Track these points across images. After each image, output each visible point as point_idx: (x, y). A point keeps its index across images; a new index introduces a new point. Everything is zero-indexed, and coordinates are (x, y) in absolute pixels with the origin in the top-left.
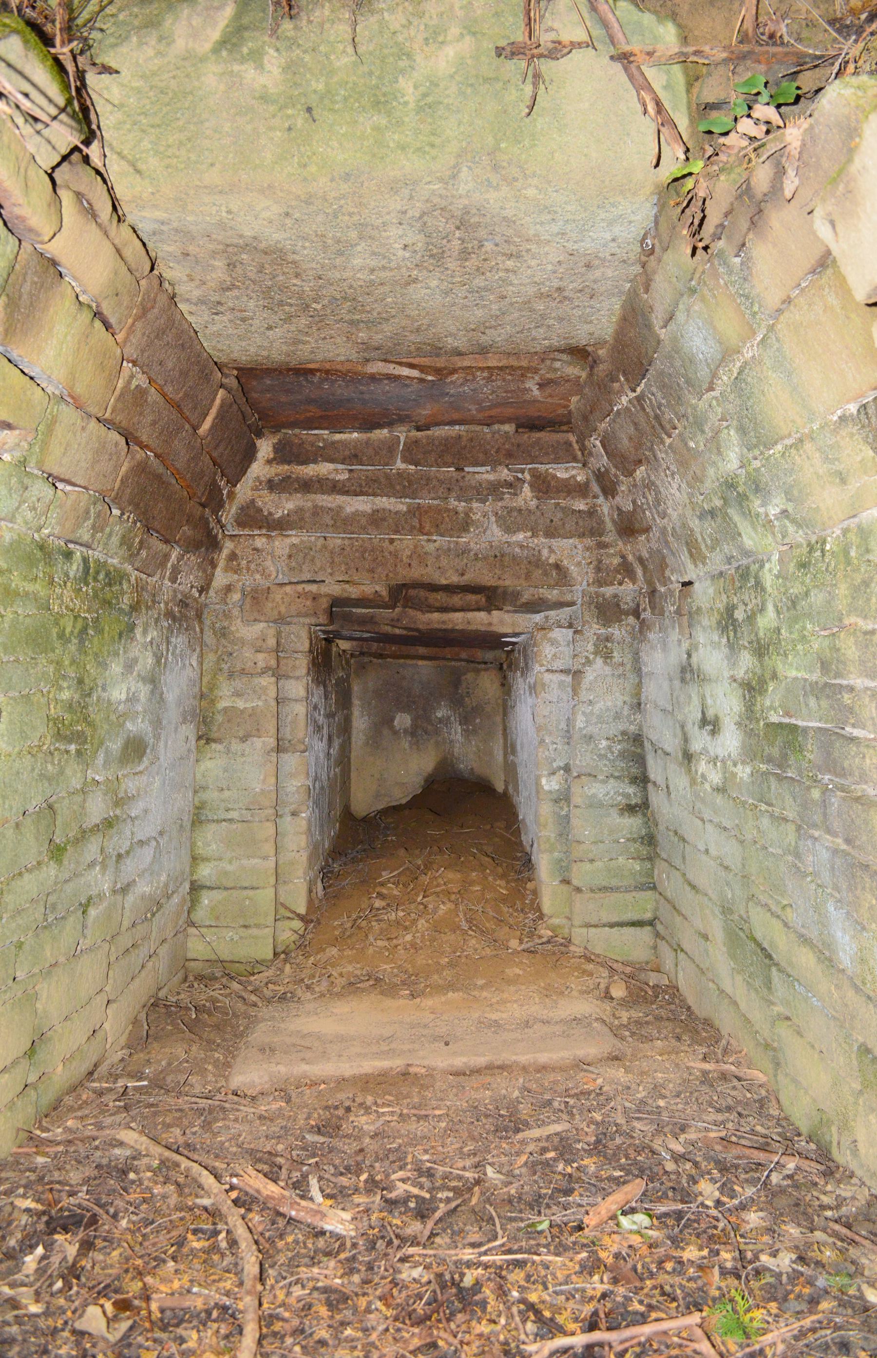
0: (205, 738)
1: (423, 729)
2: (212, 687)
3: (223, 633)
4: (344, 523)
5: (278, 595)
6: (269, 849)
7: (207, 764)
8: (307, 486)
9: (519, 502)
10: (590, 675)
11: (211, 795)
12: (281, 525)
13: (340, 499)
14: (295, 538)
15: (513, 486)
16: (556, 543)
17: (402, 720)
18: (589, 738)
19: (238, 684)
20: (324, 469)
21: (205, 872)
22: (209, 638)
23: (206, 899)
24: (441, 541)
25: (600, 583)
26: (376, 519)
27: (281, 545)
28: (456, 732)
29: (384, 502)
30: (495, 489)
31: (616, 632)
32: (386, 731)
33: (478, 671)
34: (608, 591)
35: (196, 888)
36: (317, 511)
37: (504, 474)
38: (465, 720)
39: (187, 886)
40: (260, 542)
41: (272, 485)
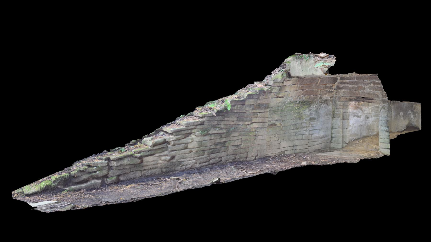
0: (333, 117)
1: (406, 116)
2: (334, 110)
3: (335, 103)
4: (349, 88)
5: (342, 98)
6: (341, 133)
7: (333, 121)
8: (344, 83)
9: (371, 86)
10: (382, 111)
11: (334, 125)
12: (341, 89)
13: (348, 85)
14: (343, 90)
15: (370, 83)
16: (377, 91)
17: (402, 114)
18: (381, 120)
19: (337, 110)
20: (346, 81)
21: (333, 135)
22: (334, 103)
23: (333, 139)
24: (362, 91)
25: (383, 97)
26: (353, 88)
27: (342, 91)
28: (412, 117)
29: (354, 85)
30: (368, 84)
31: (385, 105)
32: (398, 116)
33: (416, 104)
34: (384, 99)
35: (332, 137)
36: (346, 87)
37: (369, 82)
38: (414, 114)
39: (330, 137)
40: (339, 91)
41: (340, 83)
